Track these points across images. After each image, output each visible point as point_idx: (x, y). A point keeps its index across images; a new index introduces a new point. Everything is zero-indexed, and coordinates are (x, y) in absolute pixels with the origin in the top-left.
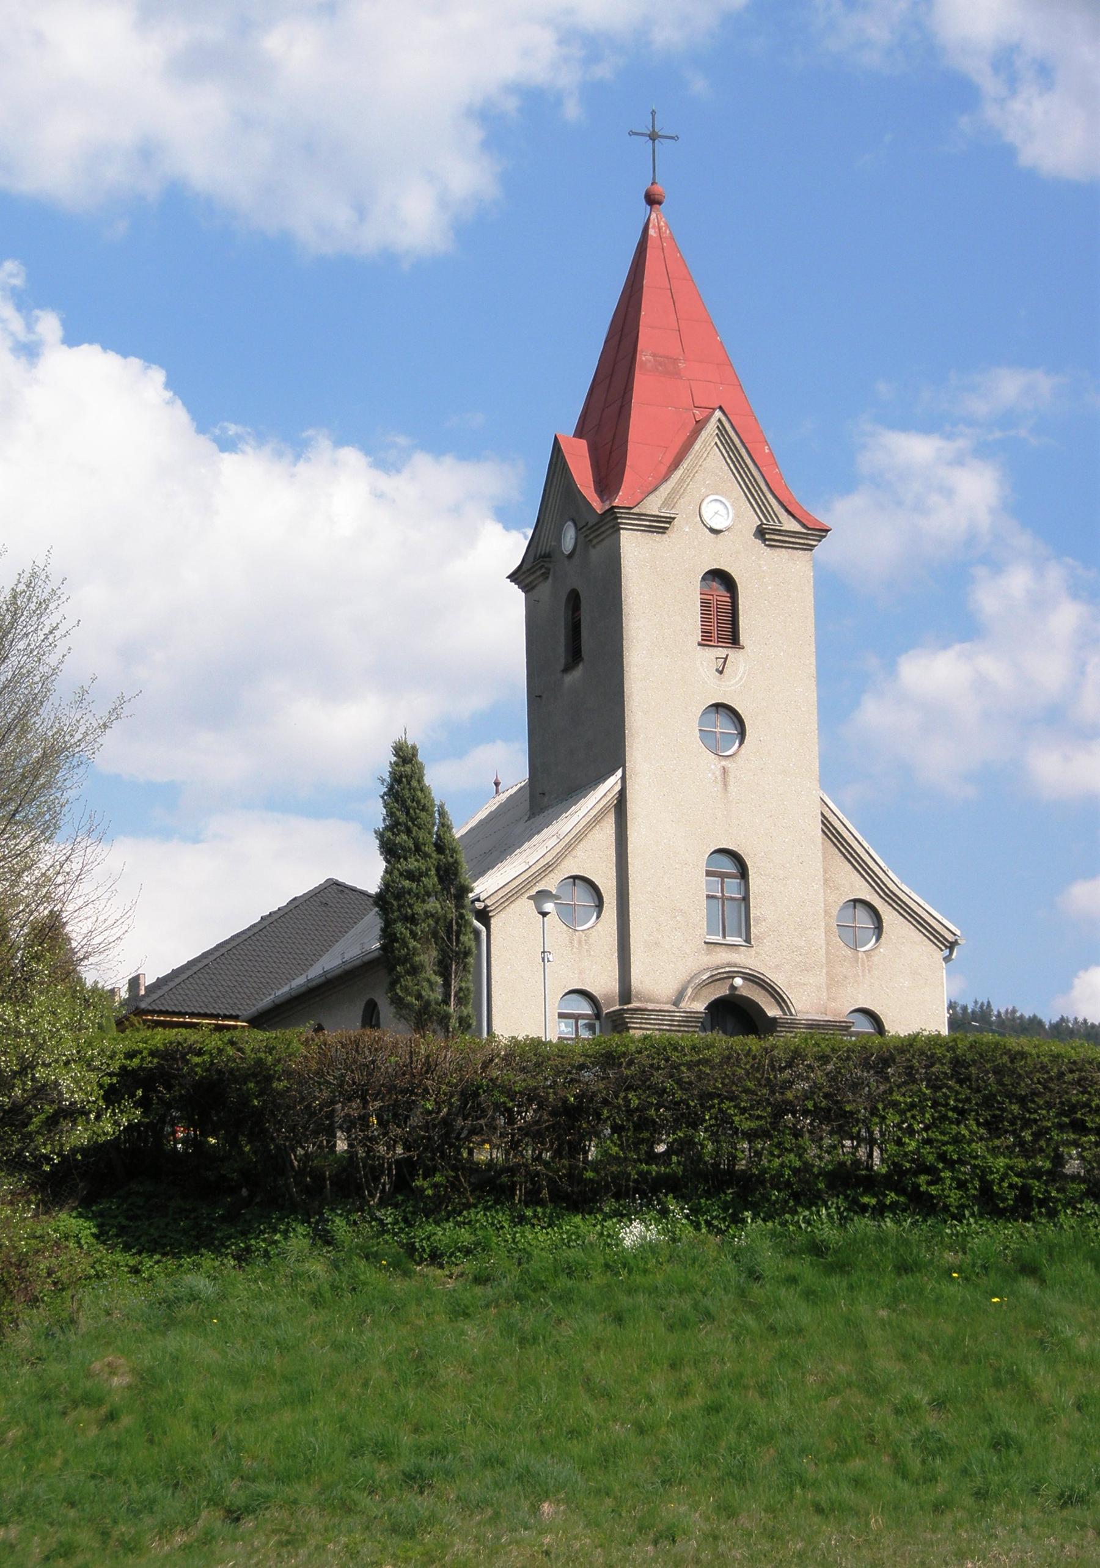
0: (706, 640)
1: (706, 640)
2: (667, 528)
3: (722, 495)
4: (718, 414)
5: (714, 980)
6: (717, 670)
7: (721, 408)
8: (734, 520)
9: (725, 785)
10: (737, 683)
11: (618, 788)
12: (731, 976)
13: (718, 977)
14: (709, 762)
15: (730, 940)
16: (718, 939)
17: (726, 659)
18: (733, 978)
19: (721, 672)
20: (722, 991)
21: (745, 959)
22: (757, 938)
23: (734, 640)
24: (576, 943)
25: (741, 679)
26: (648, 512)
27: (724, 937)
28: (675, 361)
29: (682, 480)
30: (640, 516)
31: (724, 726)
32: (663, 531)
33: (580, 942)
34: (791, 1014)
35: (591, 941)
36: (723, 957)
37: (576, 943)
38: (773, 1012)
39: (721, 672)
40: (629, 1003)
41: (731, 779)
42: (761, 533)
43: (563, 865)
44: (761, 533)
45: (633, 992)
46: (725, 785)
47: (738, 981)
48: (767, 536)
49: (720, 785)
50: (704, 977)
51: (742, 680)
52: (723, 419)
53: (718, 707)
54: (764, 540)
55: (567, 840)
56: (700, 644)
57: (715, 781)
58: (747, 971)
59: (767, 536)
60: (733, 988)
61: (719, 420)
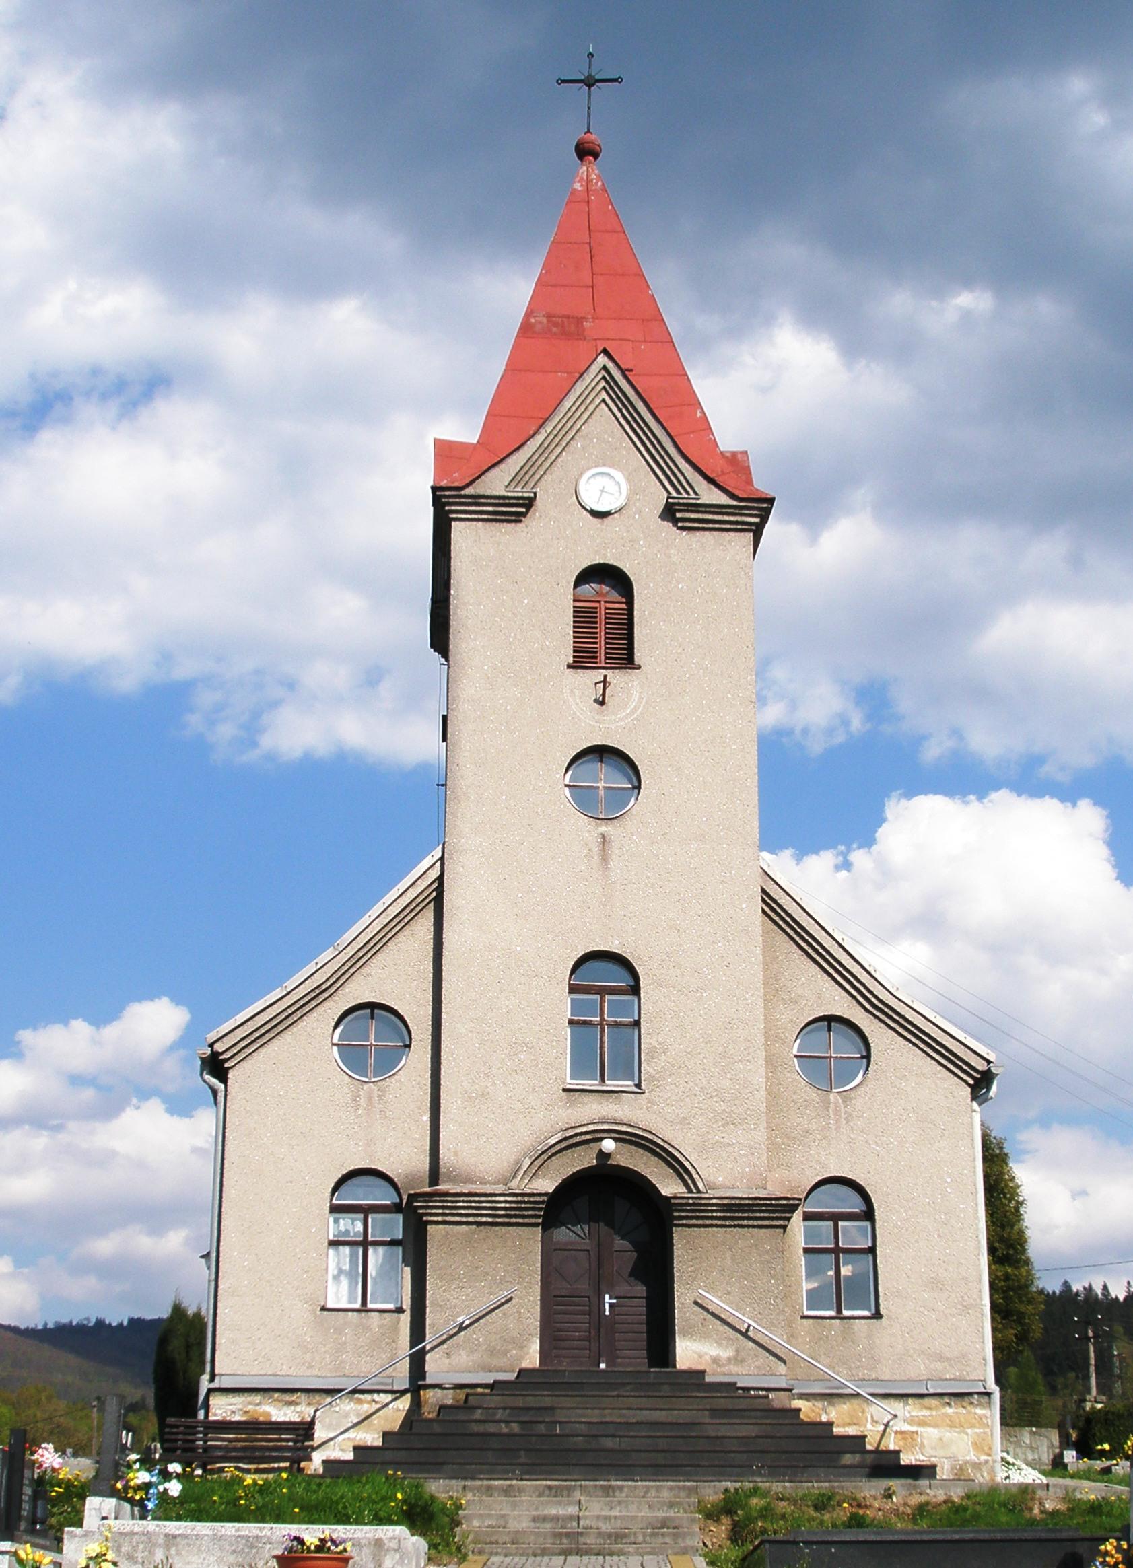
0: (582, 659)
1: (582, 659)
2: (524, 515)
3: (612, 466)
4: (602, 360)
5: (569, 1144)
6: (596, 701)
7: (605, 352)
8: (629, 498)
9: (605, 859)
10: (626, 717)
11: (434, 874)
12: (596, 1137)
13: (578, 1139)
14: (584, 829)
15: (611, 1084)
16: (593, 1084)
17: (604, 681)
18: (602, 1139)
19: (602, 703)
20: (584, 1160)
21: (628, 1111)
22: (652, 1078)
23: (625, 657)
24: (363, 1102)
25: (635, 709)
26: (488, 493)
27: (603, 1080)
28: (579, 320)
29: (543, 449)
30: (476, 499)
31: (604, 777)
32: (517, 518)
33: (370, 1098)
34: (699, 1191)
35: (389, 1097)
36: (592, 1111)
37: (363, 1102)
38: (669, 1187)
39: (602, 703)
40: (437, 1185)
41: (615, 851)
42: (670, 513)
43: (347, 989)
44: (670, 513)
45: (442, 1170)
46: (605, 859)
47: (608, 1145)
48: (678, 515)
49: (596, 858)
50: (552, 1141)
51: (631, 711)
52: (610, 366)
53: (601, 752)
54: (675, 521)
55: (350, 951)
56: (569, 666)
57: (589, 855)
58: (624, 1128)
59: (678, 515)
60: (603, 1156)
61: (605, 368)
